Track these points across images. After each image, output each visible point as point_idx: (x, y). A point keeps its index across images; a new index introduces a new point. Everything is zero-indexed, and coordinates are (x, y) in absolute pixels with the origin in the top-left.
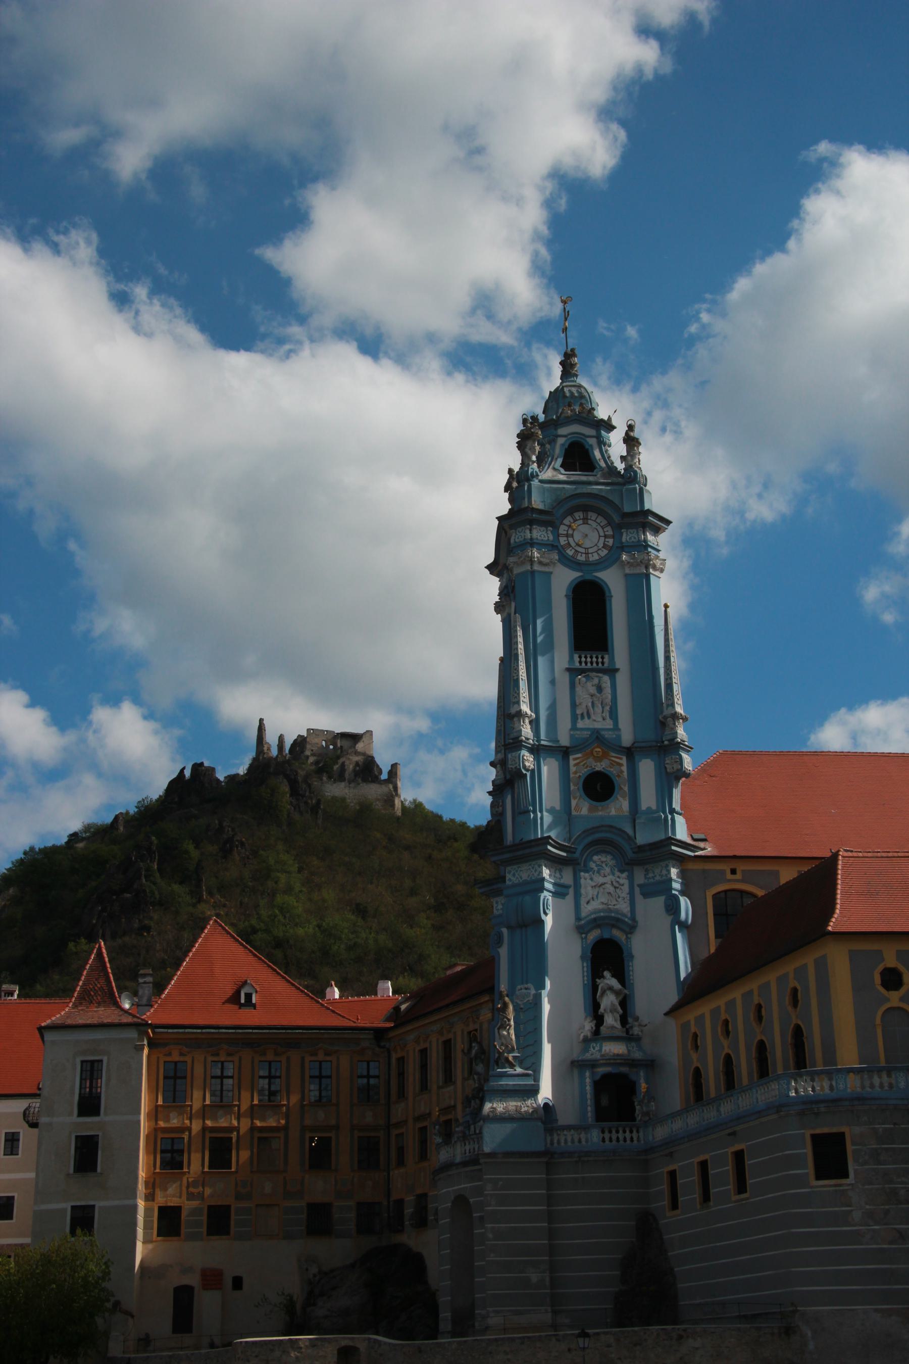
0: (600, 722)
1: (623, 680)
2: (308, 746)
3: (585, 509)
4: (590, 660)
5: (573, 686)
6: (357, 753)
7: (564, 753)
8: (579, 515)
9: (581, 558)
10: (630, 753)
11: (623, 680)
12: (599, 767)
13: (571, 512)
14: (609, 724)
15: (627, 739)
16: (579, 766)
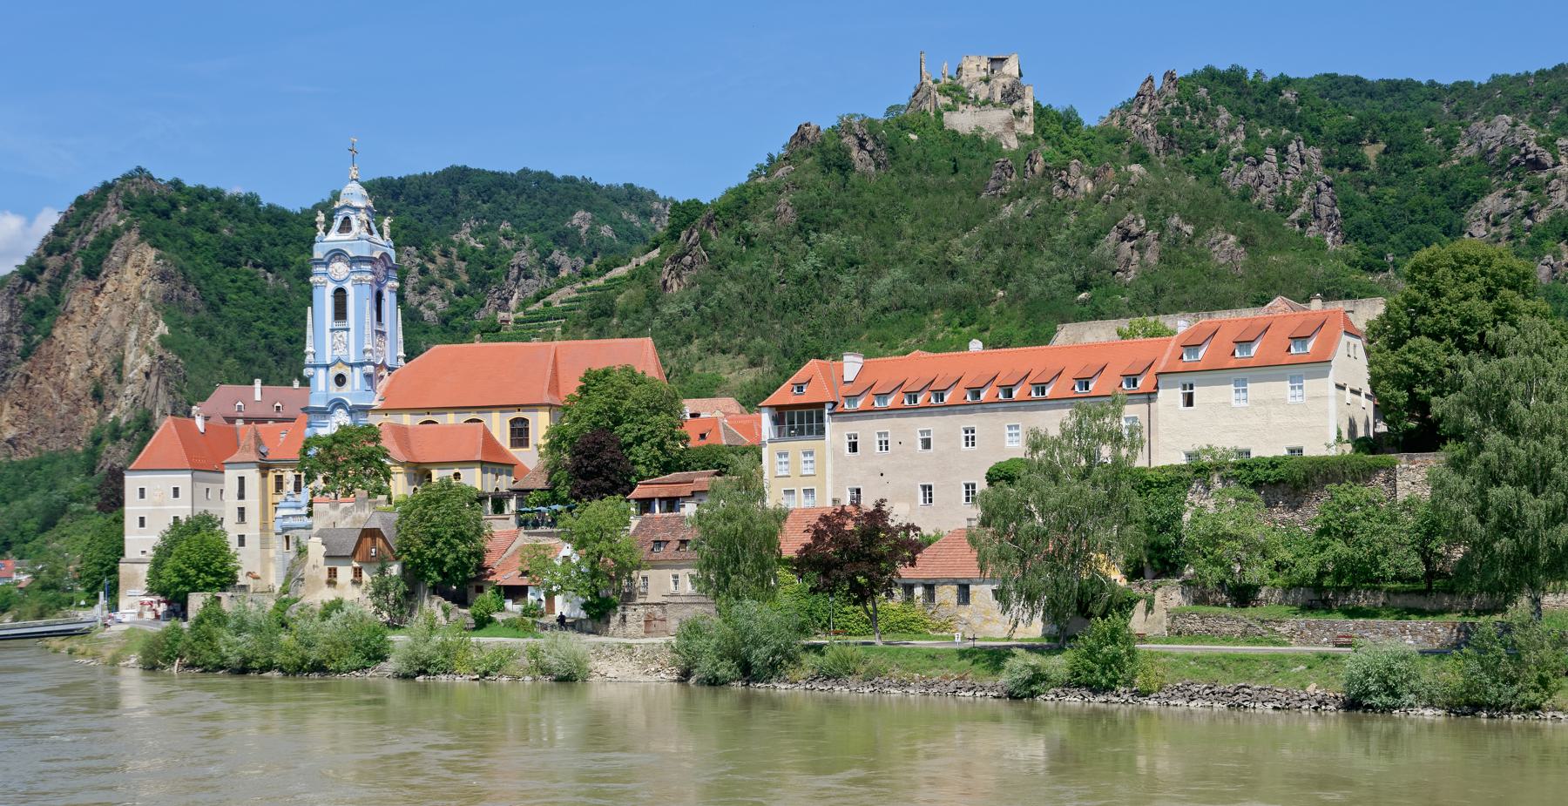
0: (339, 353)
1: (352, 332)
2: (964, 72)
3: (339, 254)
4: (340, 325)
5: (333, 337)
6: (1004, 75)
7: (327, 367)
8: (337, 257)
9: (337, 278)
10: (352, 365)
11: (352, 332)
12: (340, 371)
13: (334, 256)
14: (345, 352)
15: (352, 361)
16: (334, 372)
